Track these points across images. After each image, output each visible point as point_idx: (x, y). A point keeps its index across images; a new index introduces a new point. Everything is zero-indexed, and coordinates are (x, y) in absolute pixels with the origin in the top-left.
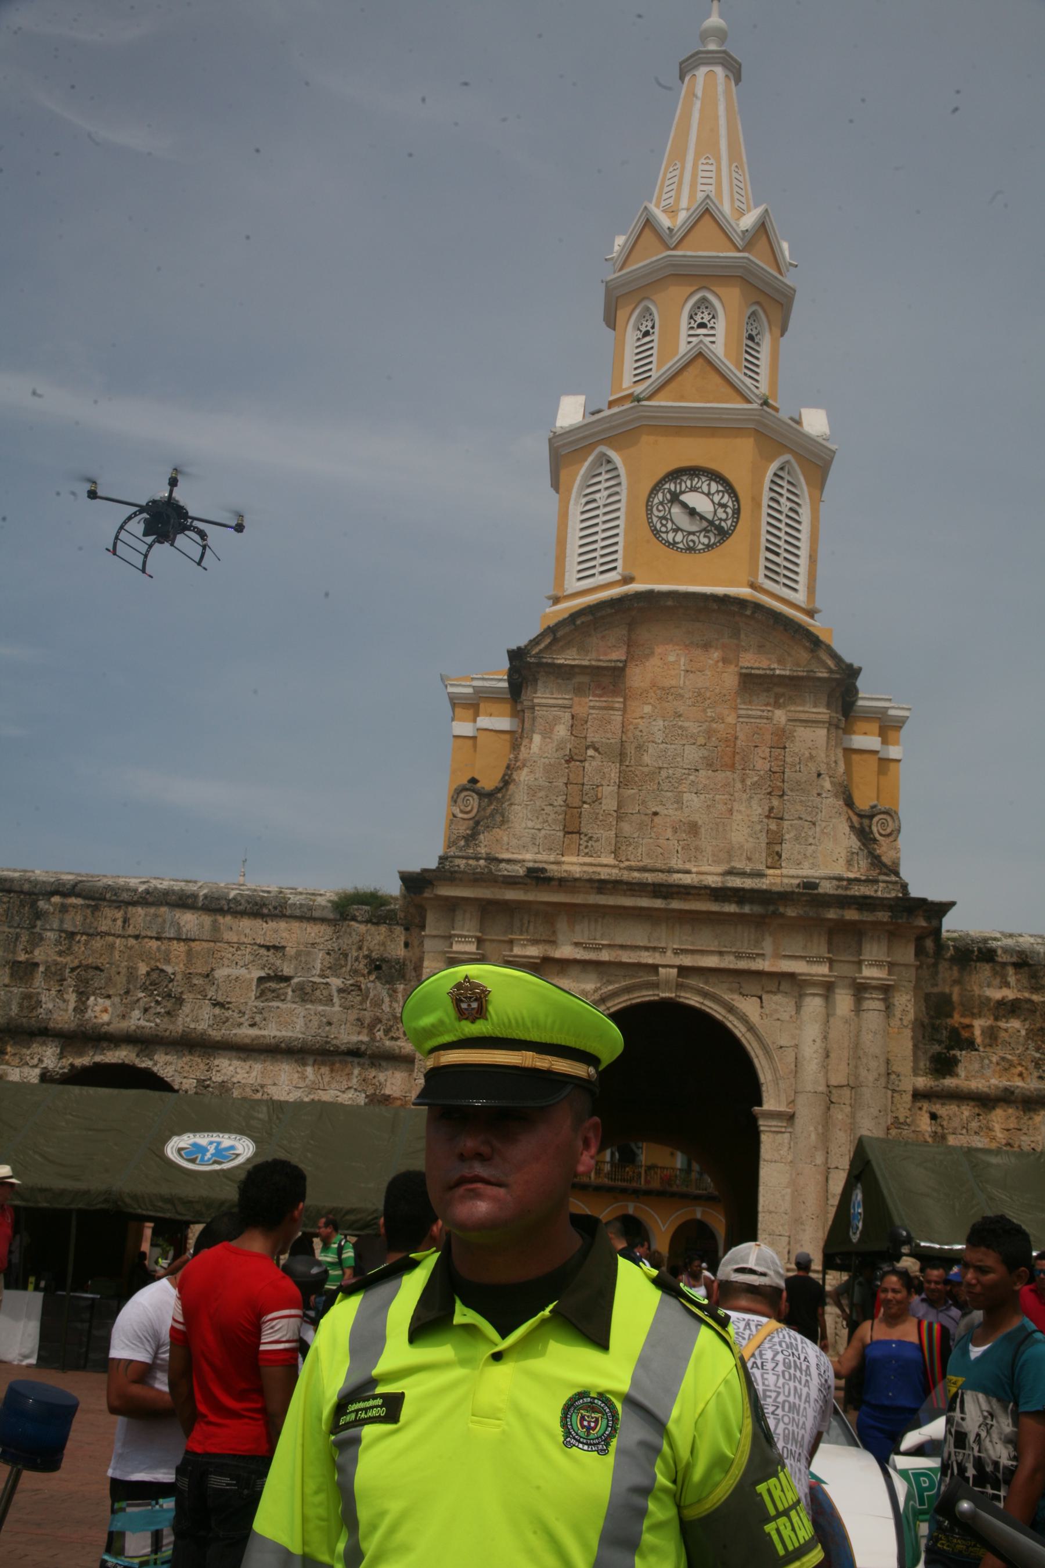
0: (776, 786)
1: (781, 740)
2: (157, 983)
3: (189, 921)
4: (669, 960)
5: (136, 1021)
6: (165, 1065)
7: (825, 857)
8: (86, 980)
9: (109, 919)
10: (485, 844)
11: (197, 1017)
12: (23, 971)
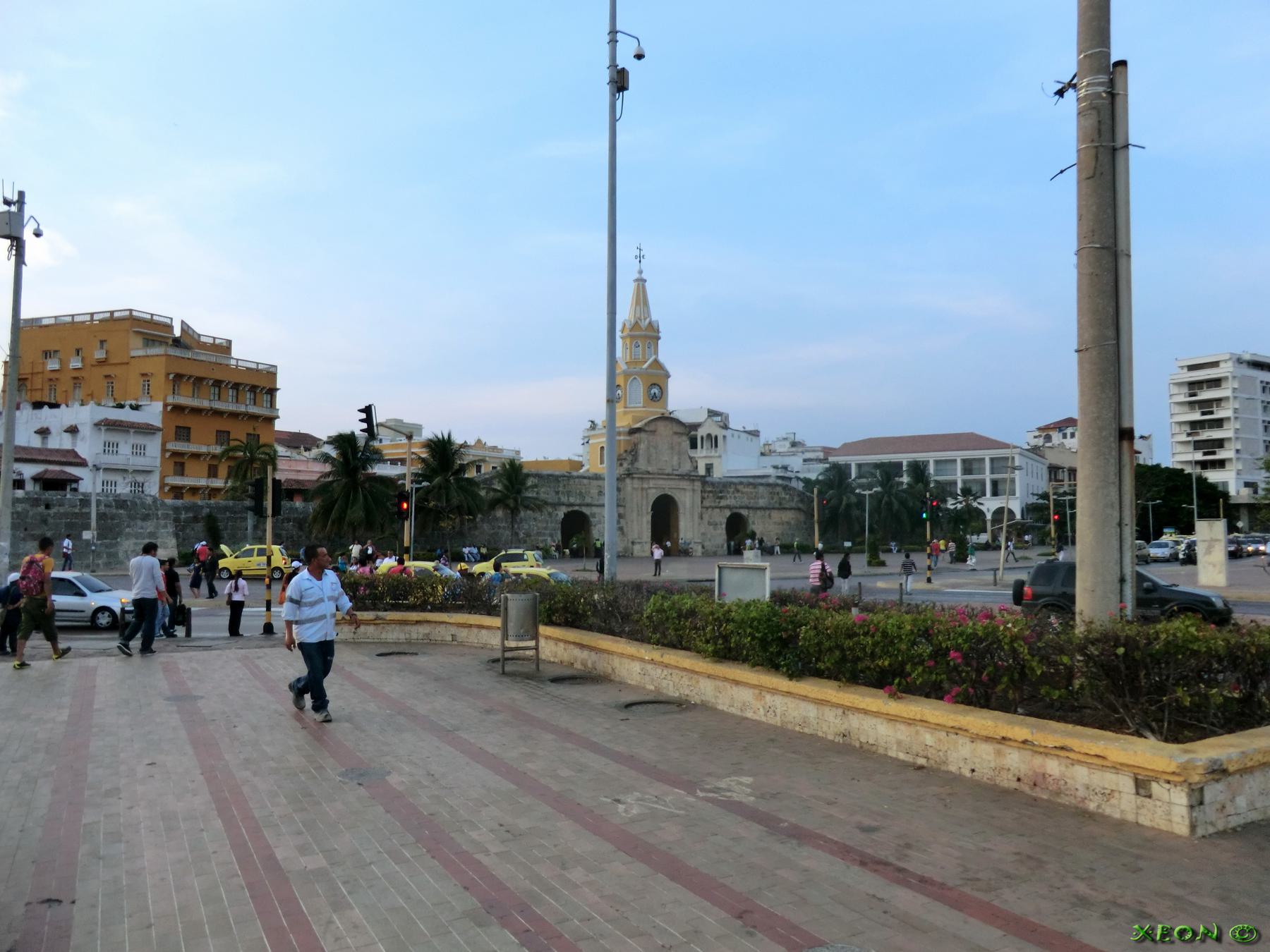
0: (679, 453)
1: (680, 444)
2: (581, 493)
3: (585, 481)
4: (667, 487)
5: (578, 502)
6: (584, 510)
7: (686, 467)
8: (569, 494)
9: (572, 482)
10: (636, 465)
11: (588, 500)
12: (557, 493)
